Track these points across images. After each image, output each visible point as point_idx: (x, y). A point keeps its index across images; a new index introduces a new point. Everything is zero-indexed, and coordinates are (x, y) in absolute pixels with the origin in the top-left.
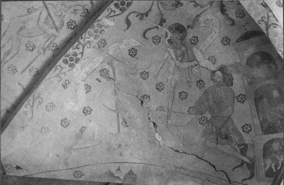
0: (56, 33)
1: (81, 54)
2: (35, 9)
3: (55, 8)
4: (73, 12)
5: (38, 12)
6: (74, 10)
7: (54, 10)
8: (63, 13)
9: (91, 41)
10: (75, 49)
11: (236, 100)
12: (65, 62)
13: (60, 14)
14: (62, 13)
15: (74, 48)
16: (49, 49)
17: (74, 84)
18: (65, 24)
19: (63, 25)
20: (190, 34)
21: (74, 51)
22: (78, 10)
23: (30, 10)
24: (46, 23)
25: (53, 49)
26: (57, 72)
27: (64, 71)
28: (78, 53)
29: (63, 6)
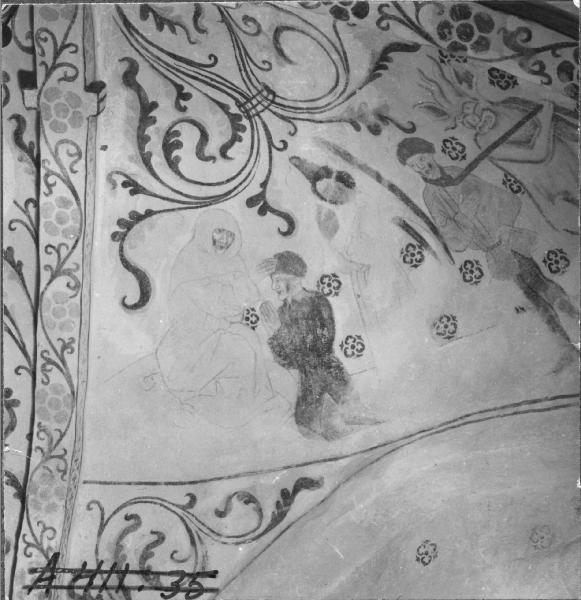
0: (545, 117)
1: (558, 52)
2: (506, 176)
3: (480, 128)
4: (467, 82)
5: (514, 169)
6: (460, 82)
7: (486, 130)
8: (483, 104)
9: (504, 37)
10: (547, 76)
13: (488, 113)
14: (484, 110)
15: (545, 80)
19: (514, 100)
23: (515, 188)
24: (528, 143)
28: (558, 61)
29: (466, 111)
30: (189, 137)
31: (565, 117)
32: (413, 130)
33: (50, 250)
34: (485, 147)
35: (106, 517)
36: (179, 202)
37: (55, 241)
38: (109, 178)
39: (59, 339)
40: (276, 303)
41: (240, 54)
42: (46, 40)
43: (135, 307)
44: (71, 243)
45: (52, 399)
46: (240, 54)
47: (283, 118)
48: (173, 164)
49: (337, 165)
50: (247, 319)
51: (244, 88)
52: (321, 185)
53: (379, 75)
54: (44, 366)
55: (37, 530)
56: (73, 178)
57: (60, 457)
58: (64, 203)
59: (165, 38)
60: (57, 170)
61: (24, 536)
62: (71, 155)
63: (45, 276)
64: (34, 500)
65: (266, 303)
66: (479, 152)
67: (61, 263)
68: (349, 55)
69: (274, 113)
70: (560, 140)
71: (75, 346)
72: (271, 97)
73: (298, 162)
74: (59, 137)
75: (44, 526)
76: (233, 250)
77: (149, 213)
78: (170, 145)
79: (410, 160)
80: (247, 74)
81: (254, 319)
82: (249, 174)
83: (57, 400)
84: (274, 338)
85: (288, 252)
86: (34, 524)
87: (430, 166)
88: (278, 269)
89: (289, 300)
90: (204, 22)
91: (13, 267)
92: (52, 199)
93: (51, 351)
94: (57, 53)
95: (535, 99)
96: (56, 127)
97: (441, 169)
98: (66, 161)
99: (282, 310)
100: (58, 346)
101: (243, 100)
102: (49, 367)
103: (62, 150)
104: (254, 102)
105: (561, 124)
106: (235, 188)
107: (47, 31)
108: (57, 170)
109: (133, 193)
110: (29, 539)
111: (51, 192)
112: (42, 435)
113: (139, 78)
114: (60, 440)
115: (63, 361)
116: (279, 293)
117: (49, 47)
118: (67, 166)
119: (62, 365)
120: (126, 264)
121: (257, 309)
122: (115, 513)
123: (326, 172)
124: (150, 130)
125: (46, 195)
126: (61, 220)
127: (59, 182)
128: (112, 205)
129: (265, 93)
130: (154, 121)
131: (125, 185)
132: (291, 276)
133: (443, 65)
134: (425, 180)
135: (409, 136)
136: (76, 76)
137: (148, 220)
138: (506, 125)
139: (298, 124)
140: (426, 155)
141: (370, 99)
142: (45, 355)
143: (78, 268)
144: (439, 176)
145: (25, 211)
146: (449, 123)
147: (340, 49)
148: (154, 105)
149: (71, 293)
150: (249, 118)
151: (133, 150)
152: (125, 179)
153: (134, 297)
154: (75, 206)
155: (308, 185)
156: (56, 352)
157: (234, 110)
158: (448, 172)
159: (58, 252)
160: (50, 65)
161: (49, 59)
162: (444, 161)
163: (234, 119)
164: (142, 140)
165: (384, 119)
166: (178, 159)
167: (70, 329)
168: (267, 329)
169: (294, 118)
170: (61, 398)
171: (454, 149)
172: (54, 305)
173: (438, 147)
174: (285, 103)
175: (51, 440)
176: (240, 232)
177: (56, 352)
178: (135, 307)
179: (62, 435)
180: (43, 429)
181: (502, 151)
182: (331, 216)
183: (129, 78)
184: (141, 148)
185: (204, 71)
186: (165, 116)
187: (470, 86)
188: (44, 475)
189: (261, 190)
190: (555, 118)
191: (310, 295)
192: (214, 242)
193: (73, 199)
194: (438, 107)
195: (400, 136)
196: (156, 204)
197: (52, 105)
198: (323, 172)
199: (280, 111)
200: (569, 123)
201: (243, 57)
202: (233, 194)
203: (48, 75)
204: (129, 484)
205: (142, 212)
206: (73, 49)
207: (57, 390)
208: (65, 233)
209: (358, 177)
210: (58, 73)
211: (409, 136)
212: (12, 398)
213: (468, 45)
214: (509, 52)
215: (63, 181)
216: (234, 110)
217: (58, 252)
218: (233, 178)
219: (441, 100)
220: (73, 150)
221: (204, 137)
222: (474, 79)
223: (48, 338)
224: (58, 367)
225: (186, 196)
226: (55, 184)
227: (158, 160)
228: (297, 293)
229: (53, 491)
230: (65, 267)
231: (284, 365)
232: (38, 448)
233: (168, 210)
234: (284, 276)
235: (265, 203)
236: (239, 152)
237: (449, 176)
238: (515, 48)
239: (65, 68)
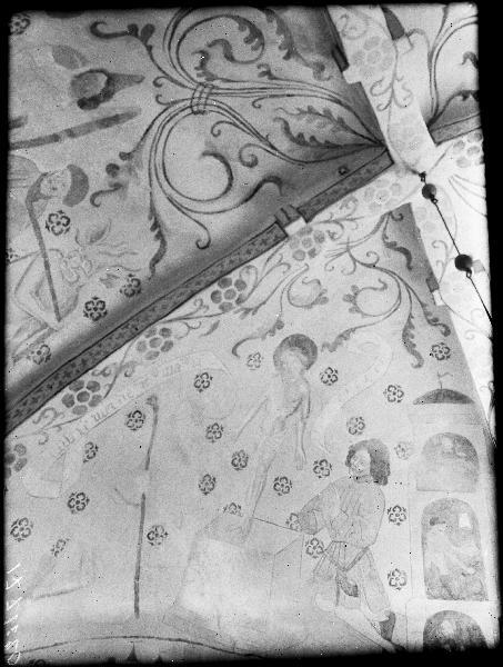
6: (108, 275)
8: (83, 280)
11: (386, 516)
12: (68, 402)
14: (79, 277)
16: (28, 358)
17: (64, 440)
18: (81, 305)
20: (324, 361)
21: (94, 379)
22: (116, 277)
25: (38, 358)
26: (45, 421)
27: (59, 421)
30: (242, 50)
31: (42, 333)
32: (92, 201)
34: (49, 254)
41: (237, 119)
46: (237, 119)
47: (175, 103)
49: (107, 108)
51: (218, 98)
52: (103, 79)
53: (150, 218)
59: (304, 104)
66: (47, 247)
68: (179, 213)
69: (183, 100)
70: (26, 318)
72: (195, 109)
73: (135, 80)
74: (368, 37)
79: (69, 173)
80: (223, 109)
82: (169, 48)
87: (54, 189)
90: (279, 125)
95: (66, 320)
97: (47, 198)
101: (214, 91)
104: (204, 95)
105: (39, 327)
123: (107, 94)
124: (280, 39)
129: (201, 108)
133: (129, 272)
134: (45, 175)
135: (90, 193)
138: (58, 285)
139: (159, 108)
140: (65, 194)
141: (137, 188)
144: (42, 192)
146: (82, 237)
147: (190, 213)
148: (287, 57)
150: (201, 84)
155: (112, 69)
157: (216, 83)
158: (41, 201)
160: (396, 82)
162: (55, 205)
163: (212, 77)
165: (117, 187)
166: (241, 29)
169: (165, 110)
171: (58, 223)
173: (65, 208)
174: (183, 114)
181: (39, 267)
182: (71, 65)
185: (257, 97)
187: (102, 280)
189: (149, 43)
190: (46, 325)
194: (99, 242)
195: (94, 187)
198: (111, 88)
199: (181, 105)
200: (35, 333)
201: (239, 123)
202: (171, 28)
206: (381, 108)
209: (86, 116)
211: (90, 193)
213: (148, 340)
214: (126, 360)
216: (216, 83)
218: (181, 40)
219: (101, 249)
221: (230, 58)
222: (104, 286)
235: (136, 35)
236: (191, 63)
237: (37, 200)
238: (127, 365)
239: (383, 89)
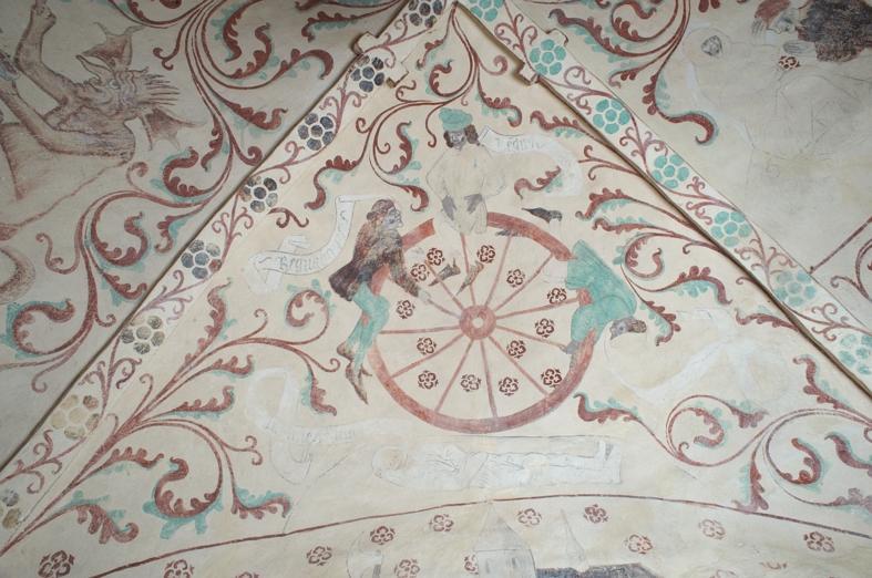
33: (624, 142)
35: (855, 280)
36: (665, 53)
37: (621, 133)
38: (613, 84)
39: (688, 186)
40: (793, 36)
42: (503, 31)
43: (709, 137)
44: (630, 124)
45: (725, 227)
48: (636, 38)
50: (787, 66)
54: (697, 213)
55: (818, 316)
56: (592, 87)
57: (775, 254)
58: (602, 106)
60: (581, 93)
61: (813, 329)
62: (578, 76)
63: (638, 160)
64: (792, 300)
65: (784, 46)
67: (638, 142)
71: (701, 180)
74: (561, 73)
75: (819, 309)
76: (726, 45)
77: (654, 79)
78: (621, 28)
81: (791, 61)
83: (729, 225)
84: (820, 54)
85: (761, 5)
86: (810, 315)
88: (767, 21)
89: (800, 25)
91: (616, 198)
92: (594, 112)
93: (692, 200)
94: (515, 31)
96: (556, 70)
98: (579, 82)
99: (804, 35)
100: (691, 191)
102: (700, 210)
103: (570, 78)
106: (685, 11)
107: (499, 26)
108: (581, 93)
109: (632, 78)
110: (820, 328)
111: (590, 109)
112: (746, 255)
113: (568, 15)
114: (761, 246)
115: (706, 197)
116: (787, 30)
117: (509, 34)
118: (583, 85)
119: (708, 200)
120: (675, 120)
121: (784, 54)
122: (858, 273)
124: (604, 34)
125: (589, 113)
126: (611, 117)
127: (587, 98)
128: (633, 91)
130: (599, 28)
131: (623, 78)
132: (781, 13)
136: (536, 31)
137: (657, 83)
142: (690, 206)
143: (651, 134)
145: (590, 159)
149: (663, 152)
151: (605, 56)
152: (619, 75)
153: (702, 133)
154: (610, 100)
156: (695, 197)
159: (630, 137)
161: (515, 40)
164: (605, 45)
166: (635, 32)
167: (687, 175)
168: (808, 53)
170: (730, 220)
172: (662, 171)
175: (757, 252)
176: (718, 31)
177: (695, 197)
178: (709, 137)
179: (759, 241)
180: (741, 252)
183: (564, 21)
184: (609, 49)
186: (602, 19)
188: (778, 278)
191: (808, 6)
192: (710, 53)
193: (605, 98)
196: (653, 70)
197: (540, 61)
203: (522, 49)
204: (843, 246)
205: (650, 83)
206: (519, 18)
207: (721, 218)
208: (622, 121)
210: (526, 40)
212: (700, 271)
215: (589, 94)
217: (630, 137)
220: (576, 72)
223: (680, 194)
224: (705, 204)
225: (664, 46)
226: (587, 102)
227: (625, 45)
228: (799, 16)
229: (795, 280)
230: (643, 141)
231: (850, 59)
232: (753, 266)
233: (663, 66)
234: (777, 18)
239: (526, 34)
